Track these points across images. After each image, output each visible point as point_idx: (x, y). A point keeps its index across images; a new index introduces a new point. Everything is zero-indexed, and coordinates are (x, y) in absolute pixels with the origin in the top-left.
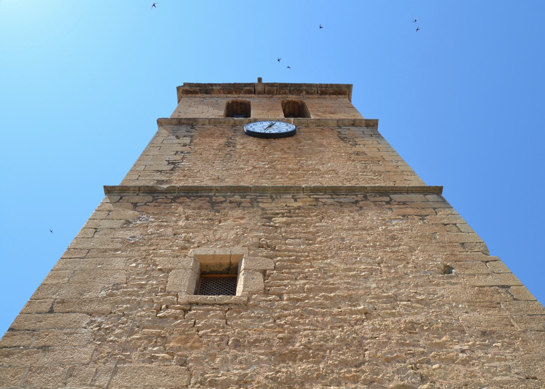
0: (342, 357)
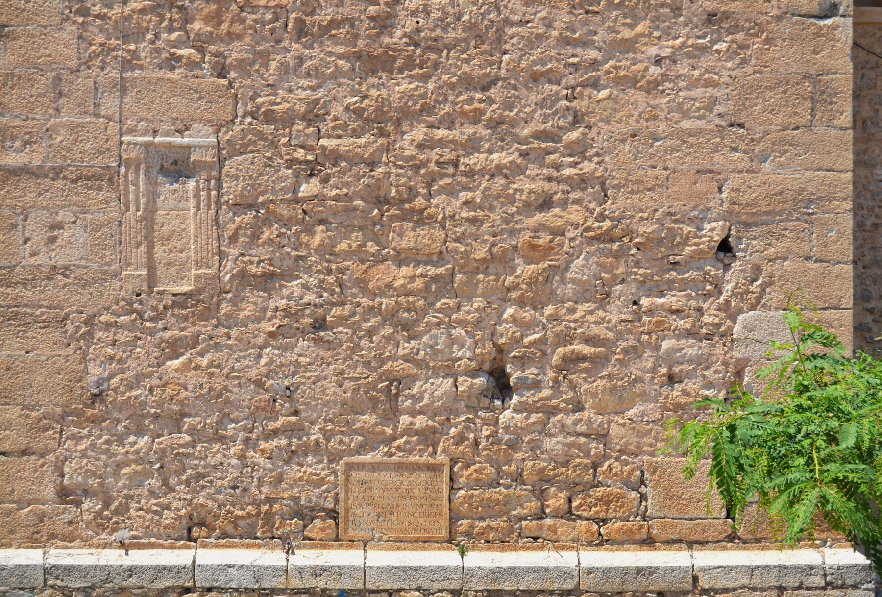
0: (466, 68)
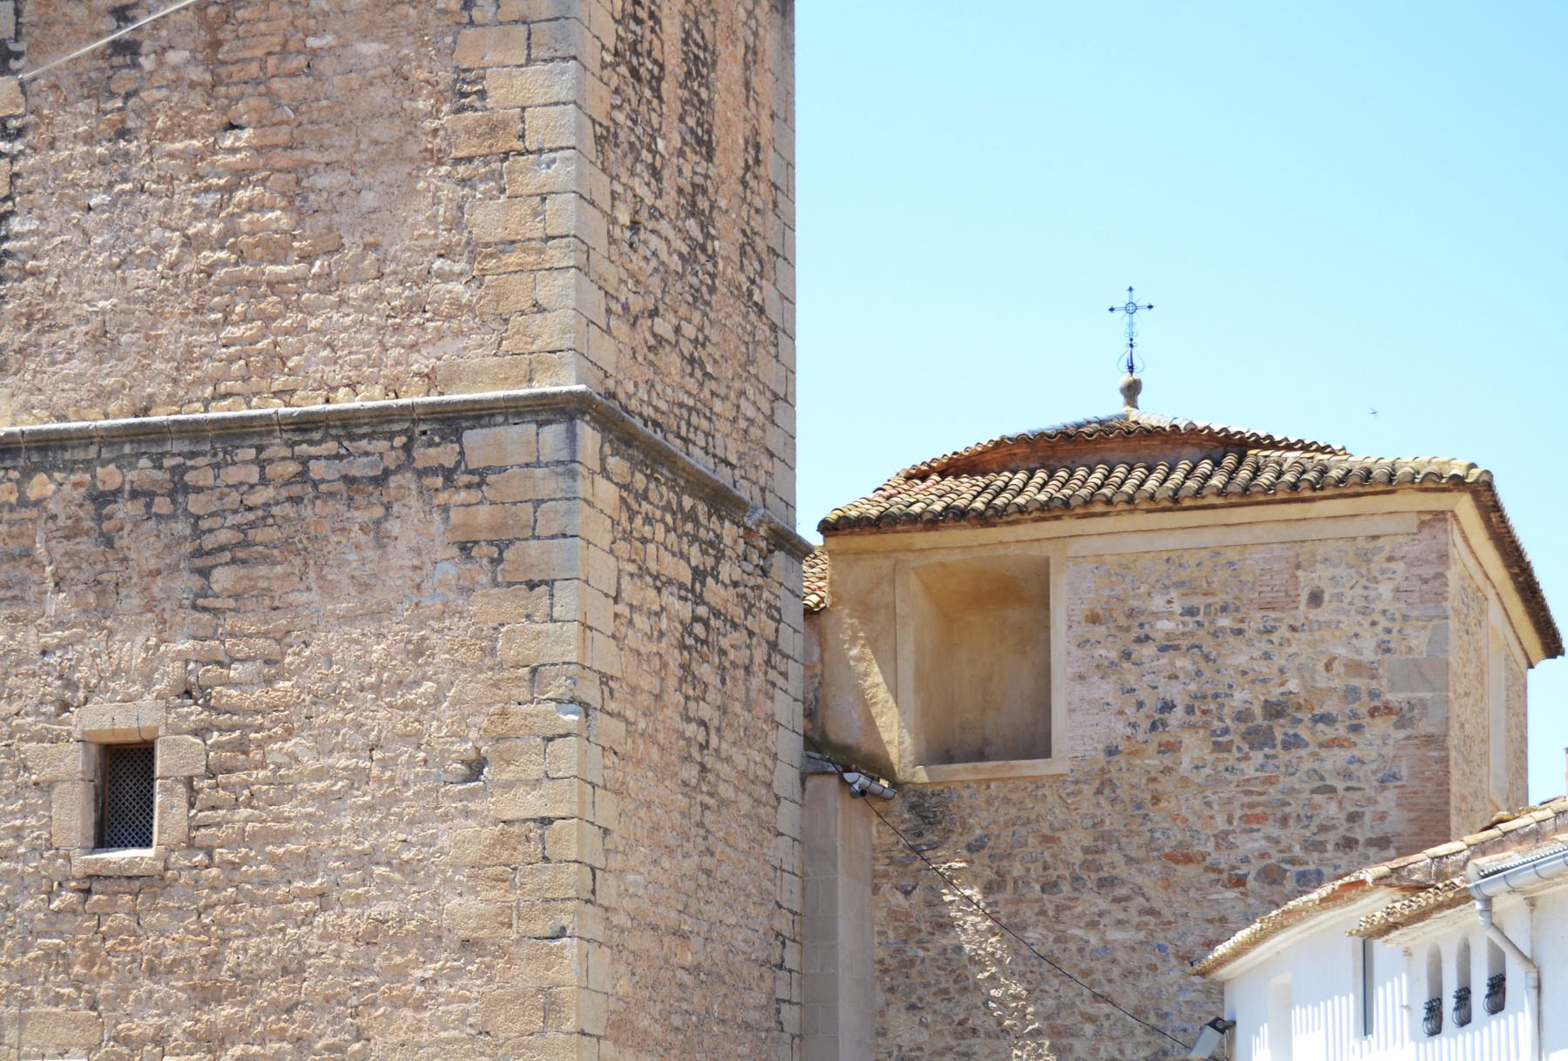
0: (274, 994)
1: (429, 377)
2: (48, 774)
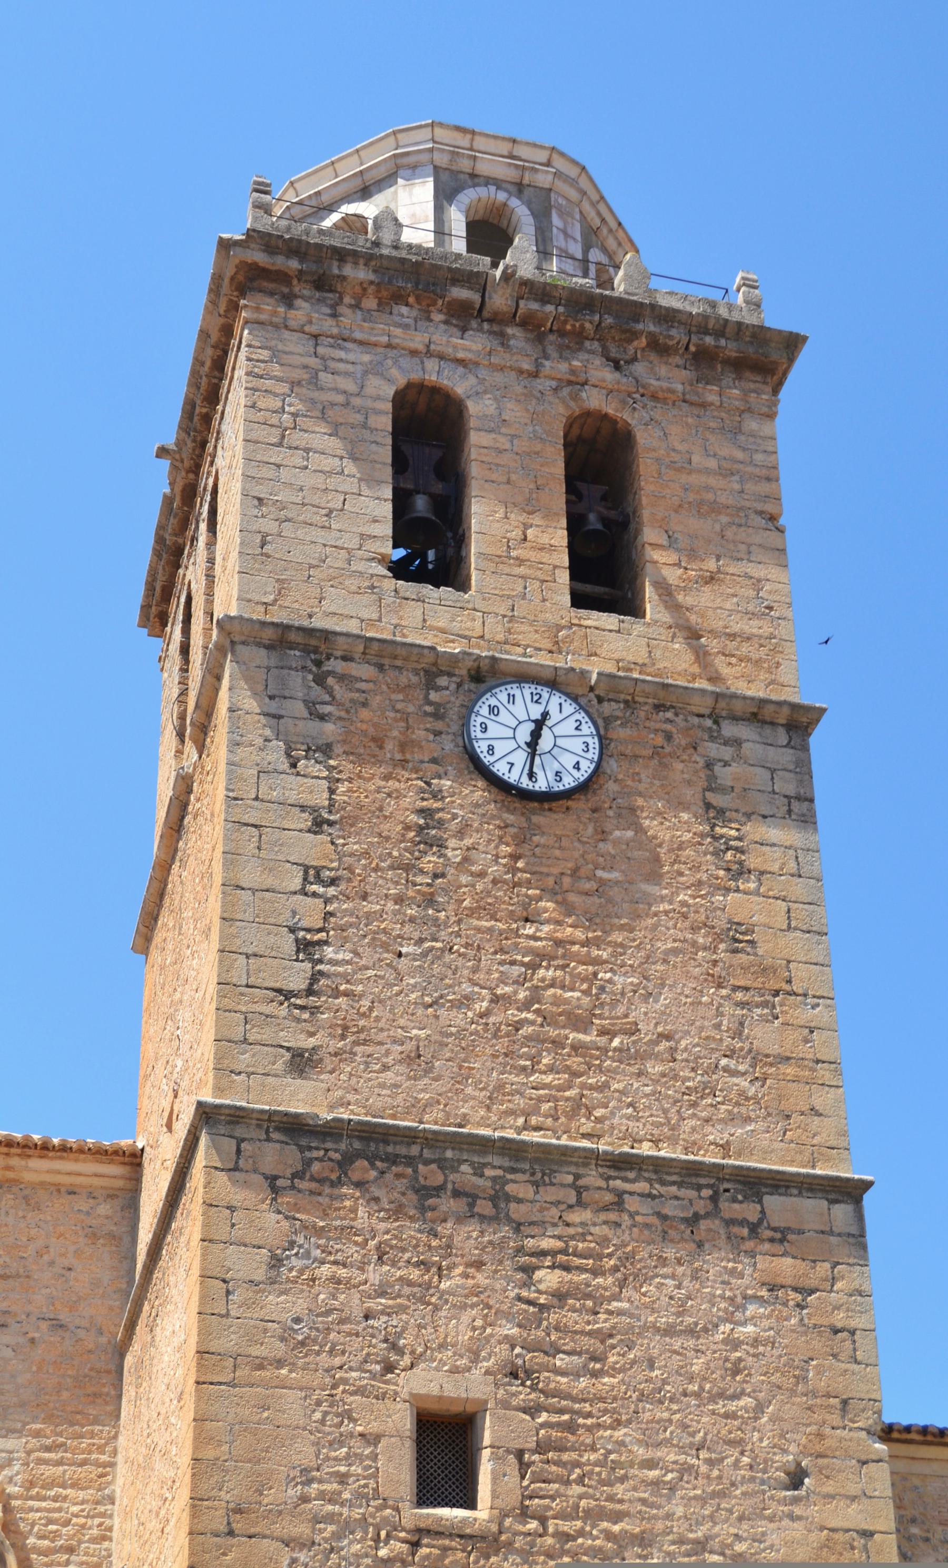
1: (725, 1148)
2: (375, 1427)
